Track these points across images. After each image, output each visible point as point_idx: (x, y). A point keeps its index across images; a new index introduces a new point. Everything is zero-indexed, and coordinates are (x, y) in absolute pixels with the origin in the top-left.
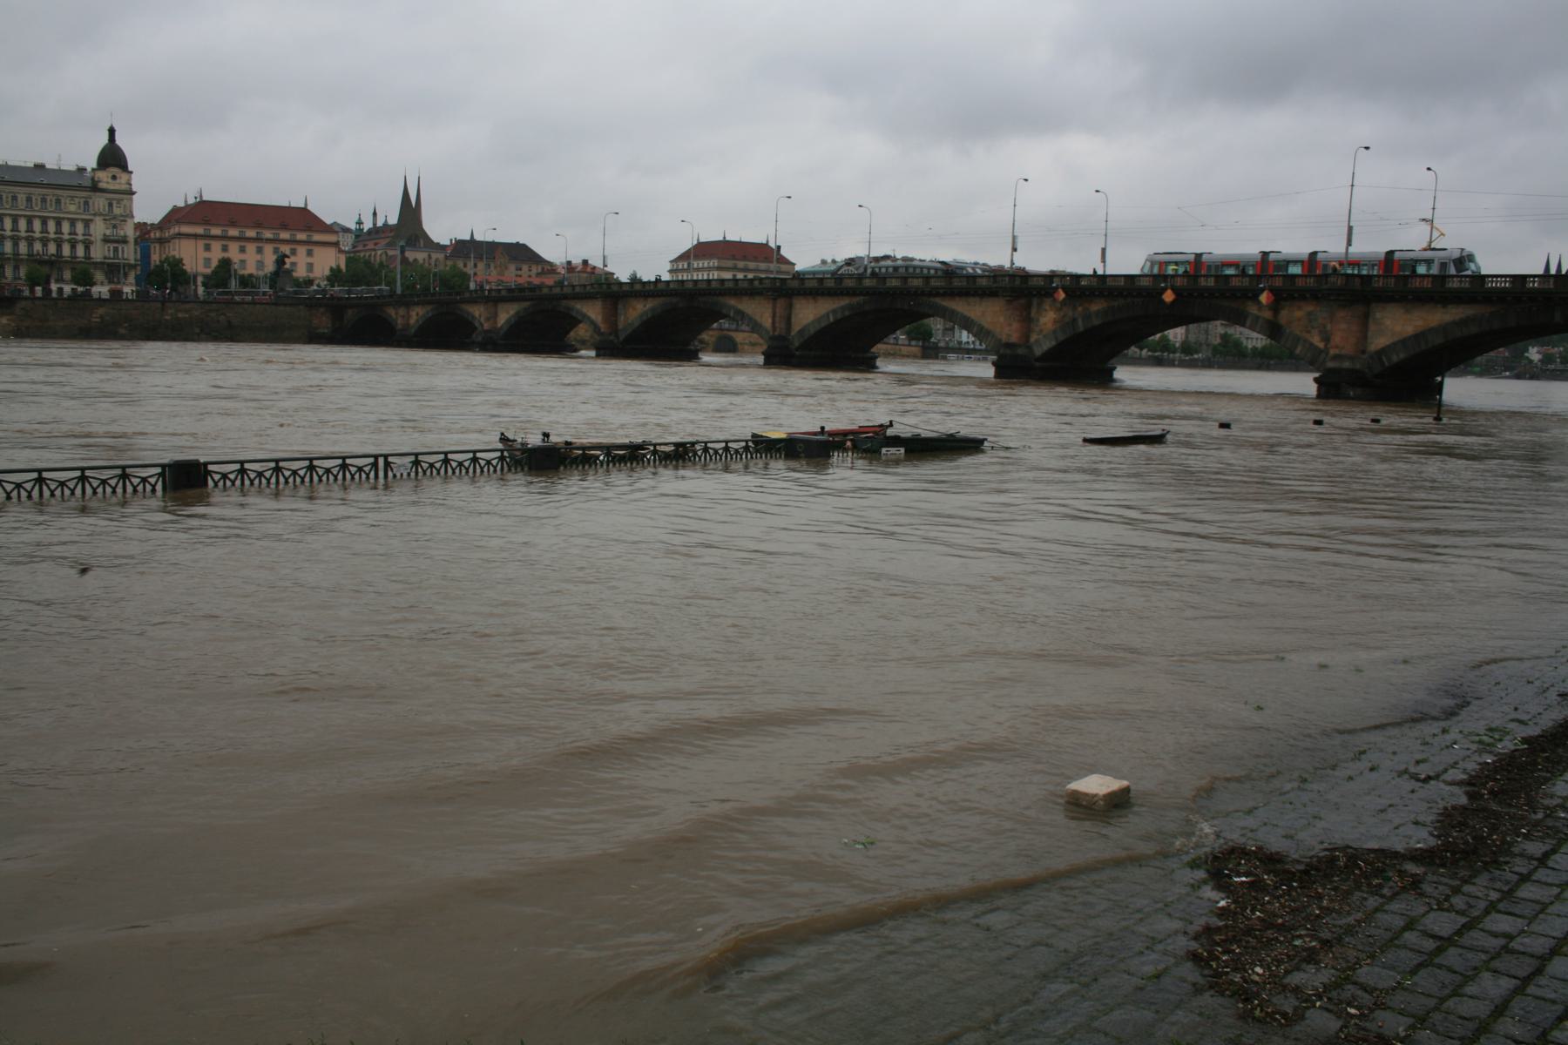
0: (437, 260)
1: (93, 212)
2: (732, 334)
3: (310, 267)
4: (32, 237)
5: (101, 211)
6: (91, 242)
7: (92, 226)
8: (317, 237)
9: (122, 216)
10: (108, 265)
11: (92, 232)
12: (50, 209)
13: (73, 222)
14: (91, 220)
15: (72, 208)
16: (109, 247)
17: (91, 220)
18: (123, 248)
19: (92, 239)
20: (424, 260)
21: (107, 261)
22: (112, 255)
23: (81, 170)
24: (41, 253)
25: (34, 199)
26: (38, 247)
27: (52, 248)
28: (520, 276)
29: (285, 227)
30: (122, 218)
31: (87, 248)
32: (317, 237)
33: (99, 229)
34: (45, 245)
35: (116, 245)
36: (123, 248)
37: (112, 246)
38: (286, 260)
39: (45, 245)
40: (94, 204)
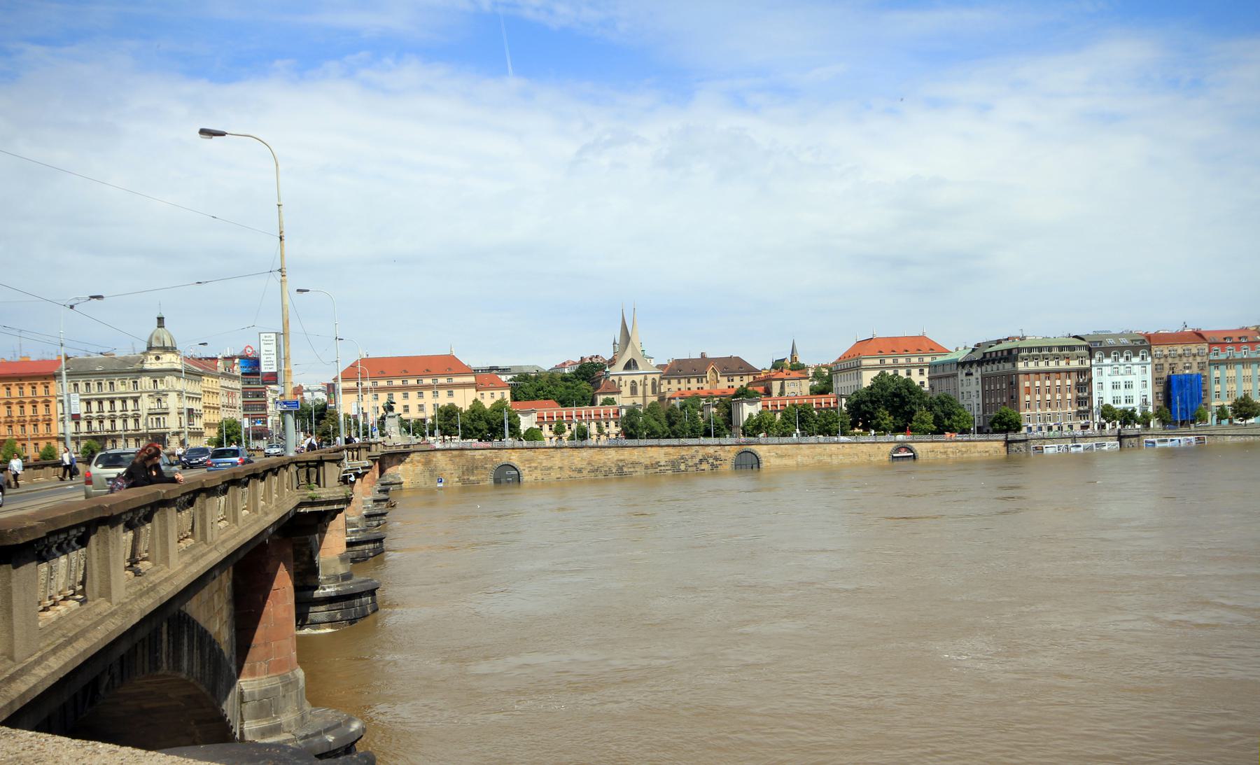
0: (654, 379)
1: (139, 390)
2: (753, 448)
3: (421, 408)
4: (90, 416)
5: (147, 388)
6: (139, 416)
7: (140, 401)
8: (456, 380)
9: (163, 391)
10: (152, 435)
11: (140, 407)
12: (106, 392)
13: (124, 401)
14: (139, 397)
15: (122, 389)
16: (152, 419)
17: (139, 397)
18: (164, 418)
19: (140, 413)
20: (641, 381)
21: (150, 431)
22: (155, 426)
23: (144, 353)
24: (98, 430)
25: (103, 384)
26: (95, 424)
27: (107, 425)
28: (733, 387)
29: (428, 373)
30: (165, 393)
31: (137, 421)
32: (456, 380)
33: (146, 404)
34: (101, 422)
35: (158, 416)
36: (164, 418)
37: (154, 417)
38: (392, 405)
39: (101, 422)
40: (141, 382)
